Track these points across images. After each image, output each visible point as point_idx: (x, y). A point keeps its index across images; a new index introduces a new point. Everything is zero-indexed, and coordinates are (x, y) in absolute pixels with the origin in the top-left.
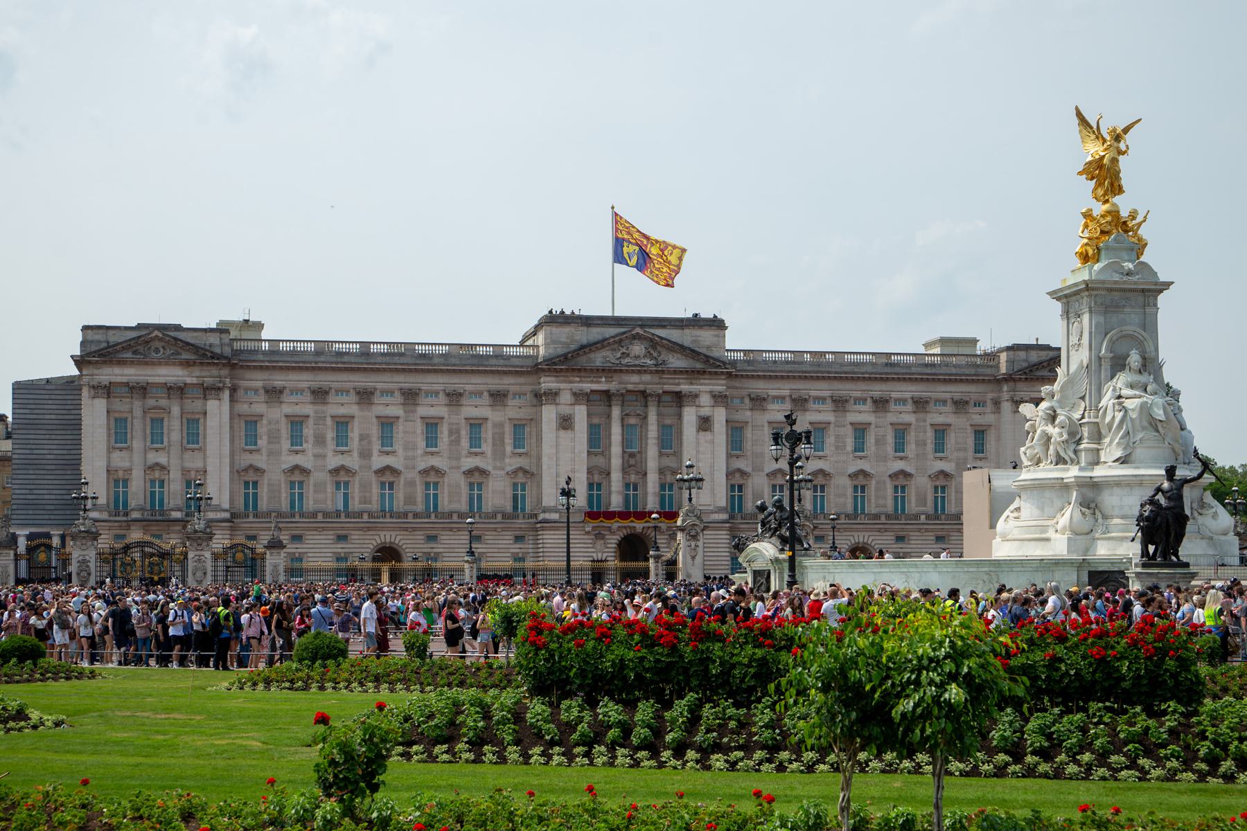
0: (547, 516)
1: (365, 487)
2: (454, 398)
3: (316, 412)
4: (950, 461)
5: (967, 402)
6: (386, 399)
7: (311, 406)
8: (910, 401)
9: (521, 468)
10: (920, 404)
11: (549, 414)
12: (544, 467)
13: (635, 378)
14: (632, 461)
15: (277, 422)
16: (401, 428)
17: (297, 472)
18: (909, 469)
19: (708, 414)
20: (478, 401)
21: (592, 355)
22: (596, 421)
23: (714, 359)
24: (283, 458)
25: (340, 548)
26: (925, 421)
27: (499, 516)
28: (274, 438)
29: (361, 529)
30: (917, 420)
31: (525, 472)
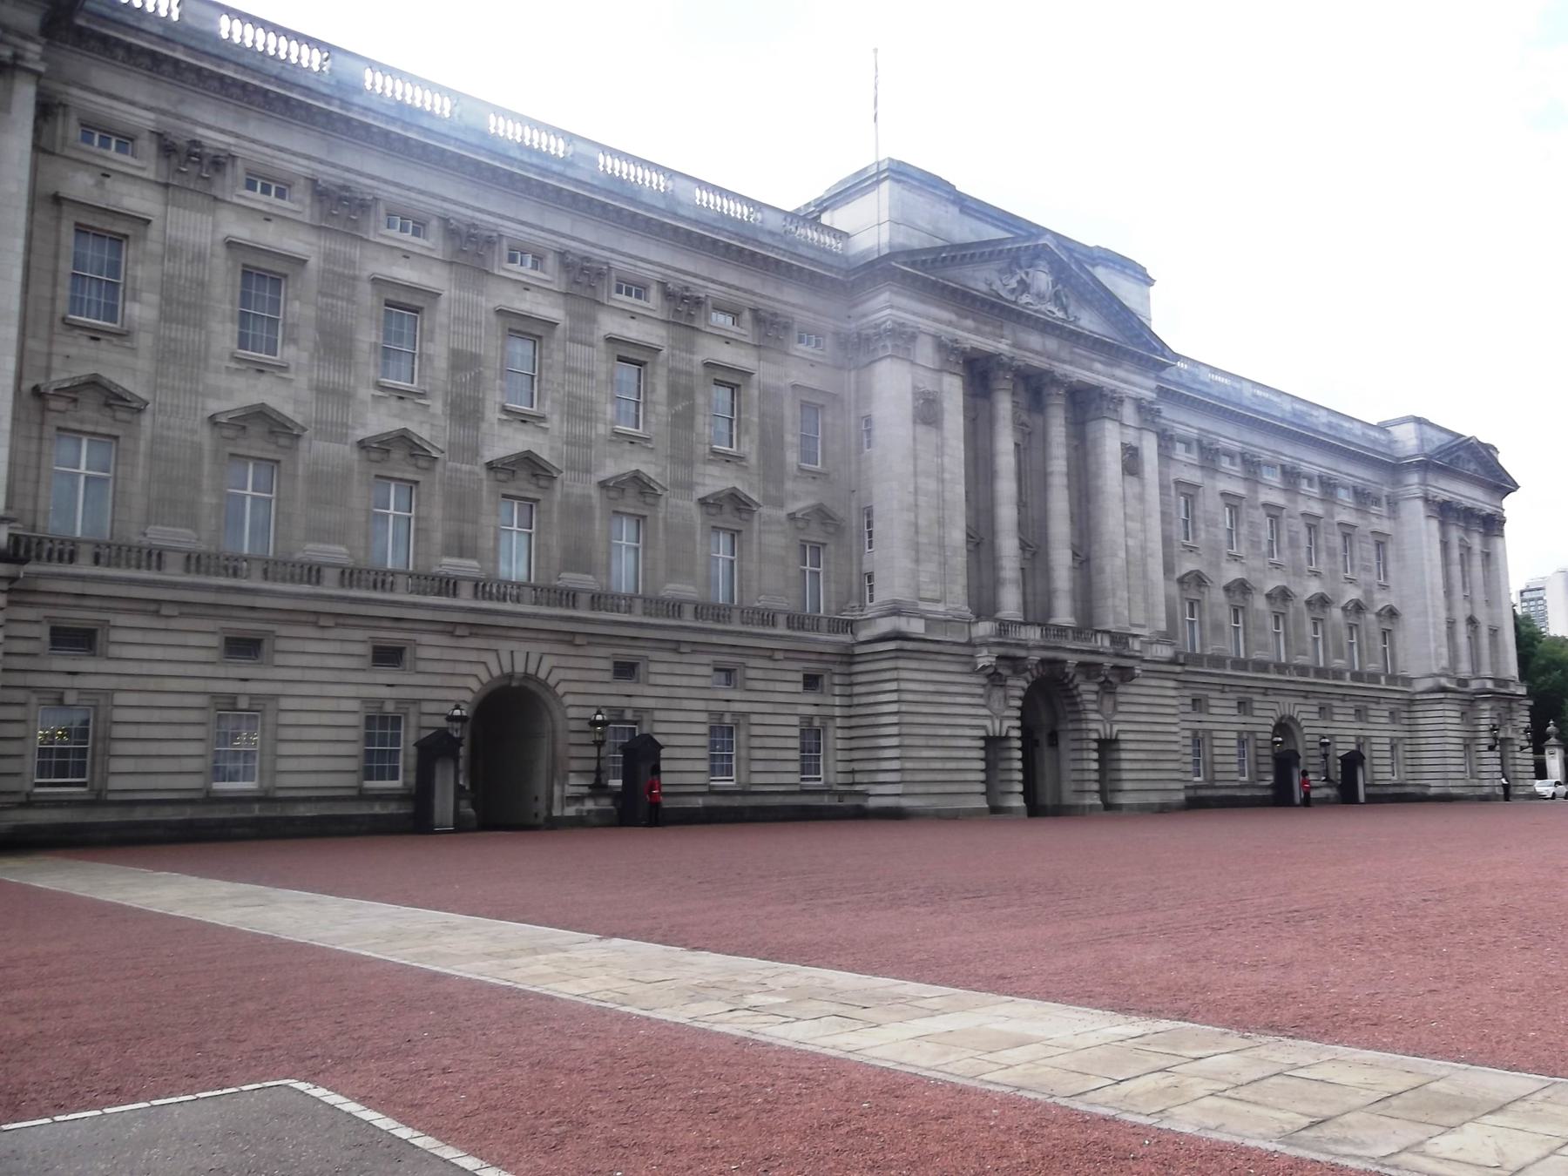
1: (461, 502)
3: (328, 257)
4: (1358, 586)
6: (523, 270)
7: (312, 238)
10: (1328, 487)
13: (1034, 340)
15: (199, 257)
16: (558, 357)
17: (256, 429)
19: (1135, 443)
21: (968, 271)
24: (212, 379)
25: (384, 685)
26: (1332, 517)
27: (781, 619)
29: (450, 629)
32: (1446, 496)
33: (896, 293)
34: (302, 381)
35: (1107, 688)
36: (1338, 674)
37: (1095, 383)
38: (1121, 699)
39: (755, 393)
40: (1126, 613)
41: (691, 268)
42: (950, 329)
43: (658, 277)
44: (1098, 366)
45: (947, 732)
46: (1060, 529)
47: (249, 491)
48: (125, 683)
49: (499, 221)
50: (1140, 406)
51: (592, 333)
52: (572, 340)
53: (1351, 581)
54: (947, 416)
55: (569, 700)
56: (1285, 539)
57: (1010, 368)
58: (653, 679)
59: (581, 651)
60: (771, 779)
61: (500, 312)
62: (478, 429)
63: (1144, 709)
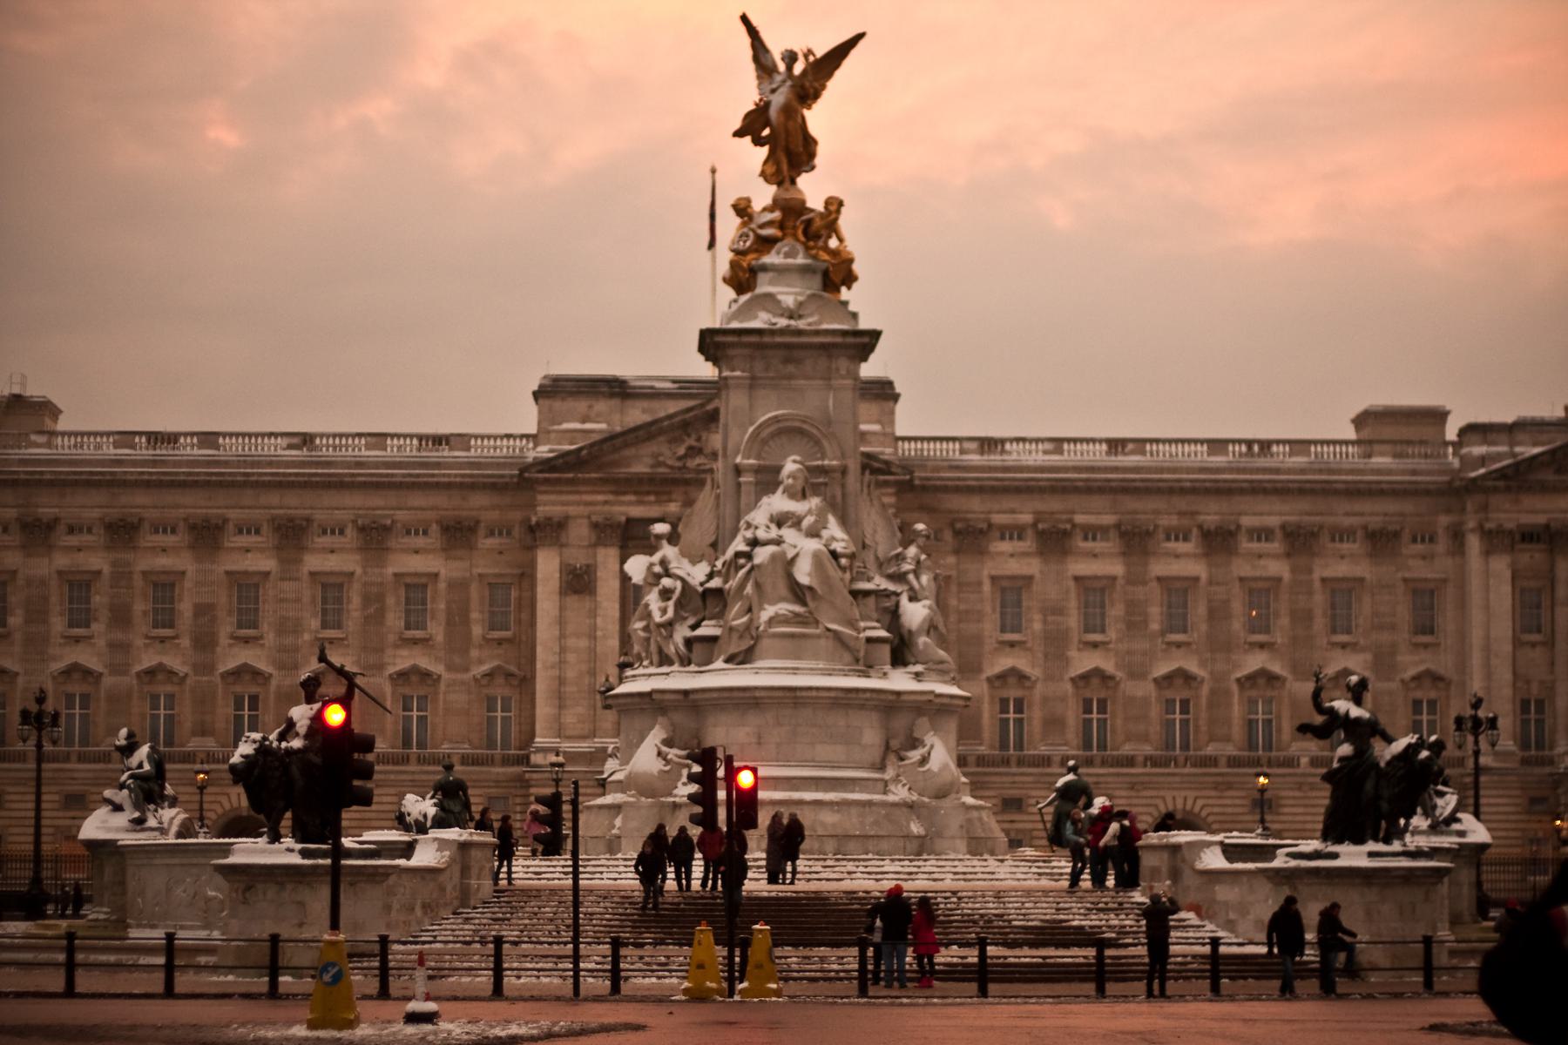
2: (375, 537)
3: (114, 564)
4: (1363, 650)
5: (1396, 535)
8: (1279, 534)
9: (499, 668)
10: (1299, 541)
12: (539, 665)
15: (43, 582)
16: (271, 593)
18: (1276, 668)
20: (420, 541)
26: (1310, 571)
28: (36, 613)
30: (1293, 571)
31: (509, 675)
32: (1541, 519)
34: (101, 643)
39: (442, 586)
42: (606, 508)
47: (77, 711)
48: (13, 822)
52: (282, 579)
53: (1344, 646)
54: (599, 583)
56: (1199, 610)
61: (227, 573)
62: (213, 652)
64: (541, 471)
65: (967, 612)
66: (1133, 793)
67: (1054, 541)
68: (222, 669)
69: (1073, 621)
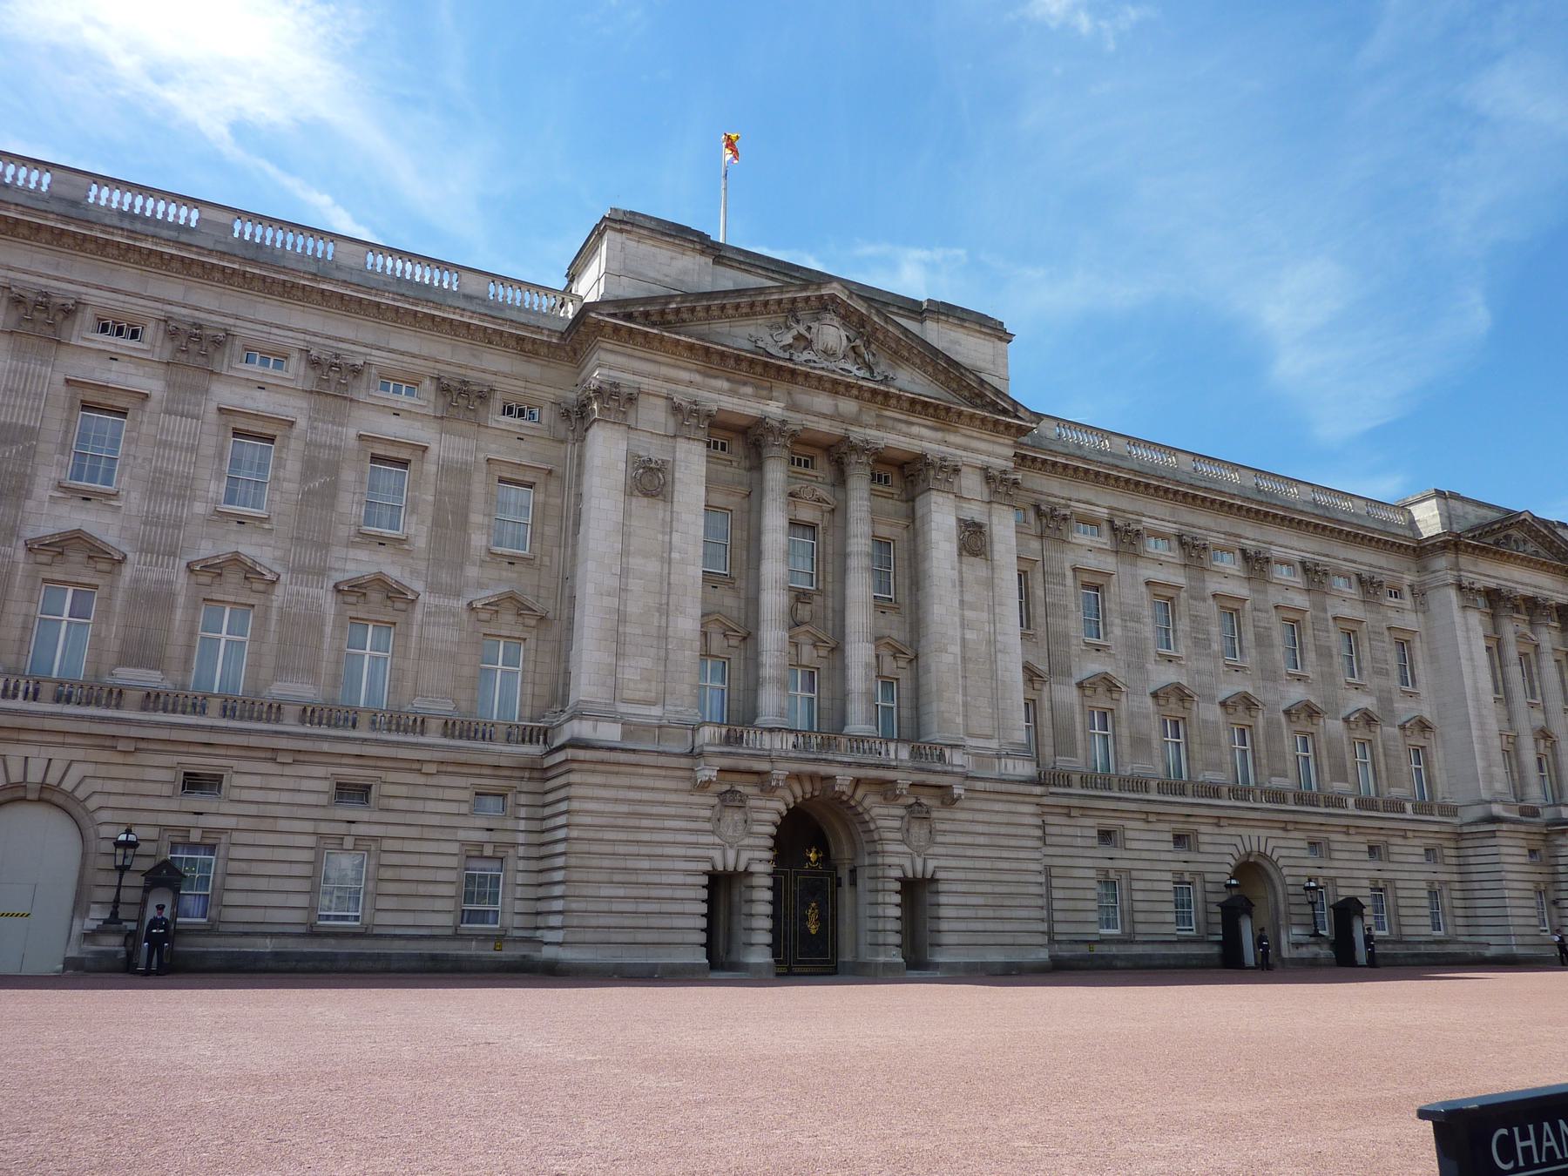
0: (583, 729)
2: (334, 377)
4: (1369, 693)
5: (1380, 584)
8: (1298, 566)
9: (511, 597)
10: (1314, 575)
11: (607, 450)
14: (804, 612)
16: (144, 429)
20: (403, 400)
22: (718, 499)
23: (997, 392)
26: (1325, 610)
27: (434, 725)
30: (1314, 605)
32: (1492, 584)
33: (611, 351)
35: (917, 813)
36: (1338, 801)
37: (918, 450)
38: (939, 826)
39: (431, 469)
40: (959, 720)
41: (351, 335)
43: (302, 345)
44: (925, 432)
45: (646, 864)
46: (859, 616)
49: (84, 289)
50: (988, 476)
51: (199, 405)
52: (168, 412)
54: (678, 486)
55: (105, 816)
56: (1249, 635)
57: (864, 450)
58: (235, 794)
59: (130, 760)
60: (408, 919)
63: (982, 840)
64: (610, 315)
65: (1054, 604)
66: (1216, 830)
67: (1126, 538)
68: (29, 534)
69: (1148, 631)
